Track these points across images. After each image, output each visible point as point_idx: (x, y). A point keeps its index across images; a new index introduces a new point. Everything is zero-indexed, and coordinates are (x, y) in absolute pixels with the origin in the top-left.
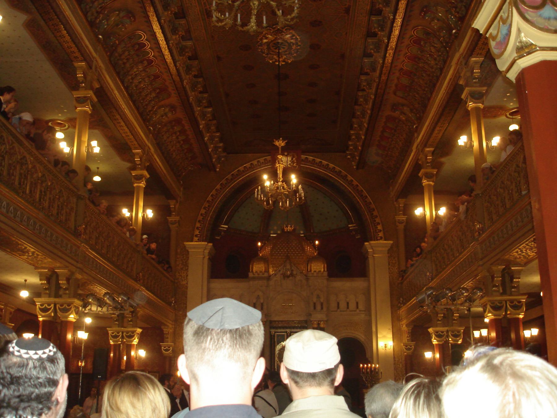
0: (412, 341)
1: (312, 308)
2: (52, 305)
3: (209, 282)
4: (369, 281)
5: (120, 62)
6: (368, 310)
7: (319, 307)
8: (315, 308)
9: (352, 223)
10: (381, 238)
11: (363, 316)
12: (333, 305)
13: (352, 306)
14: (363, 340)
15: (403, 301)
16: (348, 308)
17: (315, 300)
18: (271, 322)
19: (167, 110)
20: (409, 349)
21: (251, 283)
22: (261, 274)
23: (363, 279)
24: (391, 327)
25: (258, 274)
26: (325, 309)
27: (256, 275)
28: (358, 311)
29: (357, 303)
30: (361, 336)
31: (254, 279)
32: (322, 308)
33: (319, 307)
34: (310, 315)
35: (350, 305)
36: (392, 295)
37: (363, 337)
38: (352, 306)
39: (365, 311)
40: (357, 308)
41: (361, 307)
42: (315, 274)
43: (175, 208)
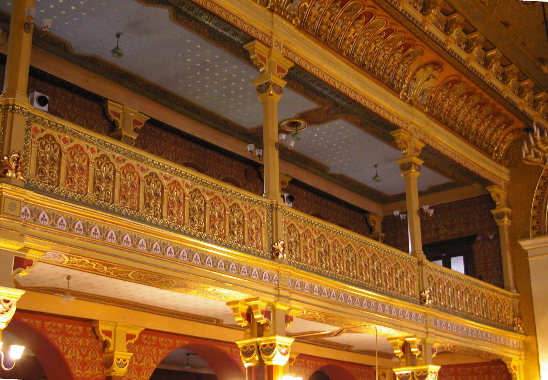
2: (256, 347)
5: (324, 27)
19: (430, 69)
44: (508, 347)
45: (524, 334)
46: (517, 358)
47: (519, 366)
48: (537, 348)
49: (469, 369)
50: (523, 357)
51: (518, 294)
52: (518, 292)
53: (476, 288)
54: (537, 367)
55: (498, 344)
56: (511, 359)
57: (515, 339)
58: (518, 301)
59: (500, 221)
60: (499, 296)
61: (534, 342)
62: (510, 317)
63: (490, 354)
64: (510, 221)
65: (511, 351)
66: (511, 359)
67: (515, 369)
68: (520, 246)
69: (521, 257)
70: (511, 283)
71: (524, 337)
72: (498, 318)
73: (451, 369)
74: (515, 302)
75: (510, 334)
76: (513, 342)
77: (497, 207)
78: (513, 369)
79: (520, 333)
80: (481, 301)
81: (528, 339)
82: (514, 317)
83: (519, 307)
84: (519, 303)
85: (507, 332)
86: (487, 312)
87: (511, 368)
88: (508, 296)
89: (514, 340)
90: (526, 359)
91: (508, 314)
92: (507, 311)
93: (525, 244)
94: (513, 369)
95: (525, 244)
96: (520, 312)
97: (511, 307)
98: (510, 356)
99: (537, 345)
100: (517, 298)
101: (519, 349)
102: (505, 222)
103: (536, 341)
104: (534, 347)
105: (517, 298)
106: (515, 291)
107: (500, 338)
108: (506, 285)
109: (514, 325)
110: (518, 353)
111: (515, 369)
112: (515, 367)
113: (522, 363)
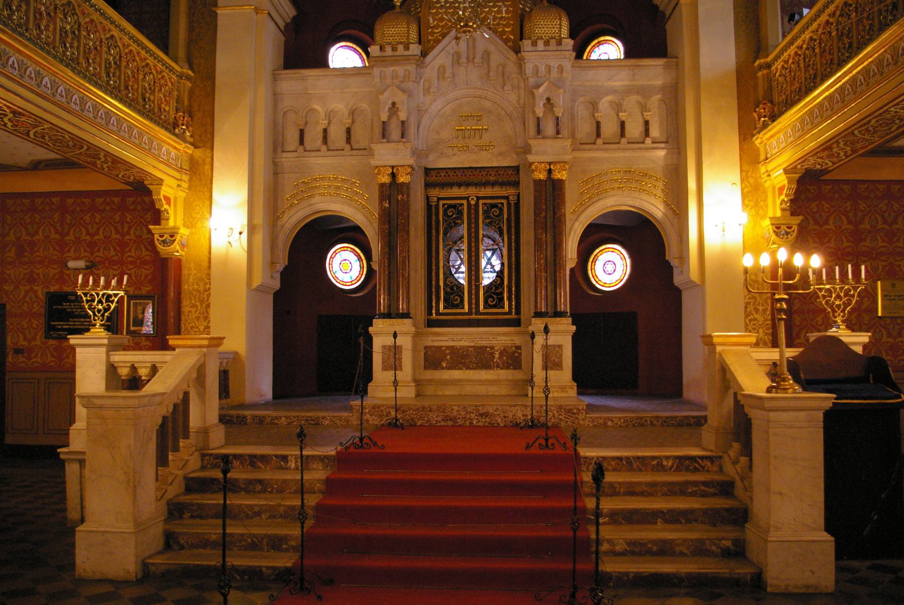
0: (793, 214)
1: (532, 131)
3: (275, 78)
6: (675, 141)
7: (549, 128)
8: (539, 131)
11: (662, 153)
12: (585, 129)
13: (634, 129)
16: (623, 134)
17: (540, 112)
18: (427, 171)
20: (787, 233)
21: (376, 71)
22: (400, 48)
23: (660, 62)
24: (736, 177)
25: (394, 49)
26: (565, 132)
28: (648, 141)
29: (647, 123)
30: (655, 207)
33: (549, 128)
34: (527, 150)
35: (628, 127)
37: (661, 207)
38: (634, 129)
39: (667, 142)
40: (647, 133)
41: (655, 132)
42: (540, 44)
44: (157, 157)
45: (192, 144)
46: (174, 183)
47: (176, 199)
48: (212, 170)
49: (87, 201)
50: (185, 185)
51: (190, 72)
52: (191, 67)
53: (96, 16)
54: (208, 203)
55: (134, 144)
56: (160, 182)
57: (175, 148)
58: (189, 84)
60: (151, 61)
61: (209, 159)
62: (170, 109)
63: (116, 161)
65: (162, 166)
66: (160, 182)
67: (169, 203)
70: (182, 53)
71: (190, 150)
72: (144, 99)
73: (54, 200)
74: (184, 84)
75: (163, 134)
76: (169, 153)
78: (164, 202)
79: (185, 141)
80: (105, 49)
81: (198, 153)
82: (177, 111)
83: (190, 99)
84: (191, 91)
85: (157, 128)
86: (119, 79)
87: (160, 200)
88: (172, 70)
89: (171, 149)
90: (190, 188)
91: (168, 103)
92: (165, 96)
94: (164, 202)
96: (190, 106)
97: (175, 93)
98: (159, 175)
99: (212, 165)
100: (188, 78)
101: (180, 170)
103: (213, 156)
104: (208, 167)
105: (188, 78)
106: (187, 66)
107: (141, 135)
109: (175, 125)
110: (177, 175)
111: (169, 203)
112: (168, 199)
113: (182, 195)
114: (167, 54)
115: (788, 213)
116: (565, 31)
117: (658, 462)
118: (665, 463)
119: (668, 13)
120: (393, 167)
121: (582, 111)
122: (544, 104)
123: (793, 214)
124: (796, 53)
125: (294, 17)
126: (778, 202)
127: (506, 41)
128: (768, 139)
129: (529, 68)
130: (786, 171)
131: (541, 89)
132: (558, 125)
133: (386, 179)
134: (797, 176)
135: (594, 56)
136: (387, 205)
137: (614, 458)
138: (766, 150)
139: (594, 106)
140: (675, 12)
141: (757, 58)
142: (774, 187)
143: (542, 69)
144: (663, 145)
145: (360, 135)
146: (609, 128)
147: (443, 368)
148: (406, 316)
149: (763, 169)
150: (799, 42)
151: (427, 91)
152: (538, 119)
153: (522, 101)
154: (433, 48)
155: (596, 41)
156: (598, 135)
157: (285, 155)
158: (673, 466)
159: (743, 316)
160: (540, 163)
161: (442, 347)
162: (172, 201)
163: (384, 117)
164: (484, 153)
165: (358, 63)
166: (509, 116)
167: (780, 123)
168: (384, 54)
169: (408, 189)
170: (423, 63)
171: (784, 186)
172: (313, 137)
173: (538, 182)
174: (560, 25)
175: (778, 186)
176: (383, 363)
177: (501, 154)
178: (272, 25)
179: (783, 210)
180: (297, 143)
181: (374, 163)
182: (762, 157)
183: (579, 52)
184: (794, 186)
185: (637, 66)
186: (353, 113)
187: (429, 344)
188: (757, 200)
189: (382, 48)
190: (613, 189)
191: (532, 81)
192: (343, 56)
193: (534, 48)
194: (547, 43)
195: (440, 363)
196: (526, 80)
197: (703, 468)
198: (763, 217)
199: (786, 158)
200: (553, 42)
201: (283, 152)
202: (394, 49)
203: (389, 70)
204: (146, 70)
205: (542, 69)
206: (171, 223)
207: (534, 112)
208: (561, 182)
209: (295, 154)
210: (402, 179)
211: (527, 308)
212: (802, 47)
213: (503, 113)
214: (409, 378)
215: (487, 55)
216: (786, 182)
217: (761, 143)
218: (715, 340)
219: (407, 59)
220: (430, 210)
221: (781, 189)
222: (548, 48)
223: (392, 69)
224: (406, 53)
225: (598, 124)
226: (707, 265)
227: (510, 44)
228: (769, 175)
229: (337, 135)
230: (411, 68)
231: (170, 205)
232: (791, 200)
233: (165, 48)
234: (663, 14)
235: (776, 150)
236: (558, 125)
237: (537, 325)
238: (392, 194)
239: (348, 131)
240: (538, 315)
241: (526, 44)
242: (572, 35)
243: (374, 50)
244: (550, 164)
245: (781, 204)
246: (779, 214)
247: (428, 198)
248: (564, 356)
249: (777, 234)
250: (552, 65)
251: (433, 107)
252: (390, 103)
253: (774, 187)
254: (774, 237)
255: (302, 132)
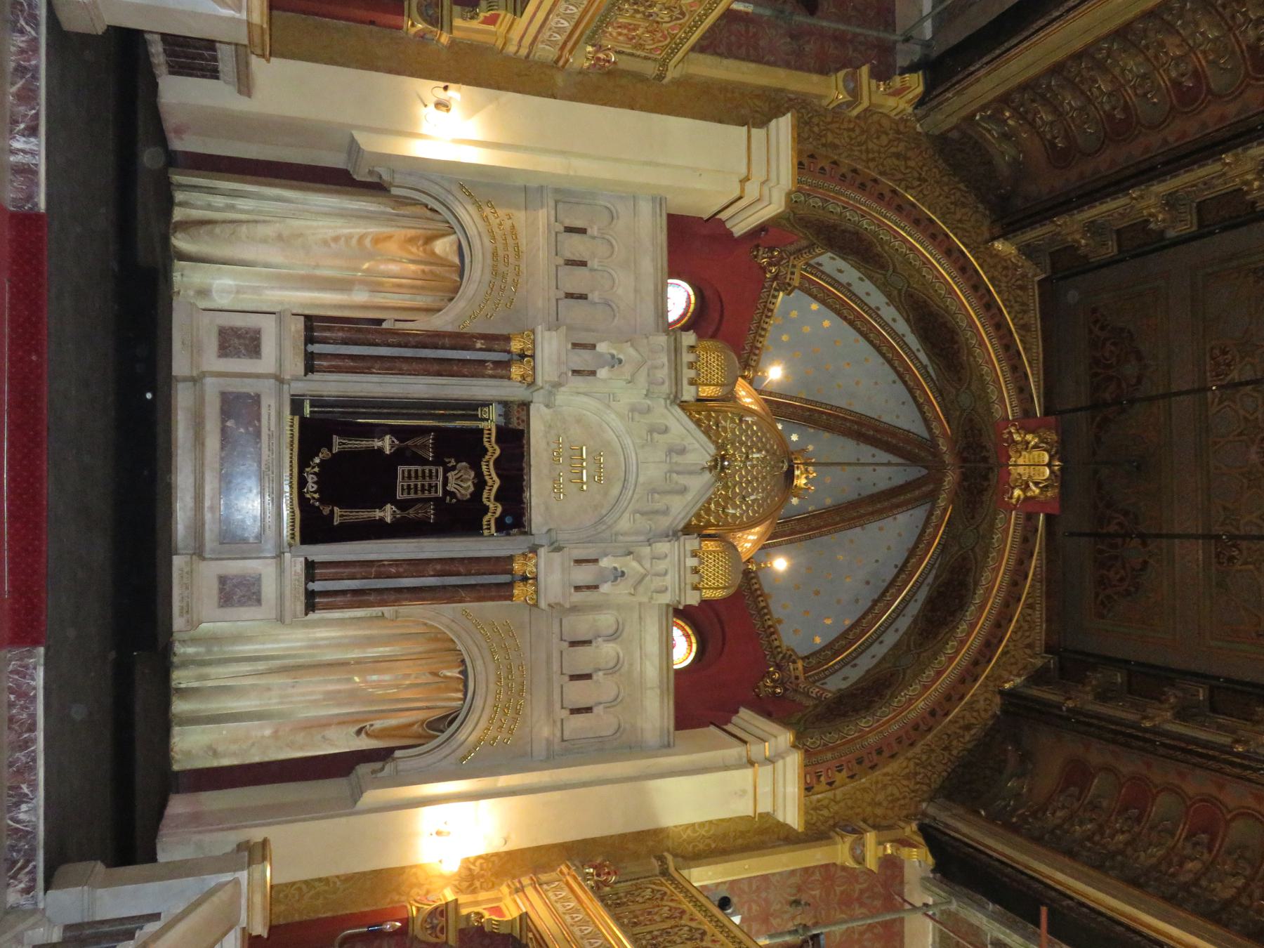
0: (462, 933)
4: (667, 746)
6: (565, 752)
7: (583, 575)
9: (806, 670)
10: (809, 789)
11: (546, 732)
12: (581, 626)
13: (578, 693)
14: (461, 736)
15: (605, 883)
16: (574, 677)
17: (605, 563)
18: (525, 405)
22: (692, 373)
24: (513, 845)
25: (691, 365)
27: (687, 357)
28: (565, 713)
29: (588, 710)
31: (677, 350)
32: (578, 588)
33: (583, 575)
36: (623, 836)
37: (472, 738)
38: (578, 693)
39: (563, 740)
40: (576, 711)
43: (898, 93)
59: (841, 84)
64: (831, 106)
68: (778, 112)
69: (751, 110)
77: (874, 82)
78: (488, 14)
93: (783, 126)
95: (783, 126)
100: (660, 77)
102: (834, 93)
108: (692, 55)
114: (693, 49)
115: (462, 926)
116: (708, 594)
117: (26, 795)
118: (24, 807)
119: (729, 727)
120: (533, 356)
121: (606, 620)
122: (615, 569)
123: (462, 933)
124: (683, 912)
125: (732, 233)
126: (479, 909)
127: (698, 516)
128: (567, 884)
129: (663, 547)
130: (524, 917)
131: (635, 564)
132: (588, 587)
133: (516, 346)
134: (516, 933)
135: (677, 633)
136: (478, 345)
137: (33, 716)
138: (552, 882)
139: (614, 636)
140: (734, 740)
141: (675, 856)
142: (499, 899)
143: (661, 566)
144: (558, 734)
145: (576, 311)
146: (582, 659)
147: (223, 421)
148: (310, 368)
149: (526, 881)
150: (699, 916)
151: (633, 409)
152: (596, 561)
153: (621, 538)
154: (690, 416)
155: (690, 632)
156: (574, 644)
157: (552, 203)
158: (18, 822)
159: (305, 878)
160: (536, 565)
161: (259, 421)
162: (492, 28)
163: (602, 347)
164: (549, 485)
165: (672, 317)
166: (601, 520)
167: (591, 900)
168: (684, 350)
169: (502, 377)
170: (673, 402)
171: (502, 915)
172: (575, 246)
173: (511, 559)
174: (717, 589)
175: (501, 905)
176: (232, 328)
177: (547, 508)
178: (725, 201)
179: (468, 916)
180: (568, 223)
181: (539, 329)
182: (544, 877)
183: (684, 614)
184: (504, 930)
185: (662, 693)
186: (607, 304)
187: (265, 402)
188: (483, 876)
189: (692, 348)
190: (498, 668)
191: (646, 550)
192: (679, 297)
193: (688, 554)
194: (695, 571)
195: (229, 418)
196: (649, 542)
197: (14, 877)
198: (459, 890)
199: (544, 920)
200: (696, 578)
201: (556, 202)
202: (691, 365)
203: (664, 359)
204: (677, 12)
205: (661, 566)
206: (458, 22)
207: (606, 555)
208: (510, 597)
209: (553, 219)
210: (516, 371)
211: (323, 552)
212: (692, 920)
213: (604, 512)
214: (206, 368)
215: (683, 490)
216: (508, 918)
217: (561, 872)
218: (257, 868)
219: (677, 381)
220: (471, 408)
221: (497, 911)
222: (689, 571)
223: (665, 360)
224: (685, 382)
225: (588, 642)
226: (386, 814)
227: (694, 522)
228: (517, 891)
229: (575, 280)
230: (666, 388)
231: (483, 22)
232: (481, 928)
233: (700, 48)
234: (728, 721)
235: (553, 898)
236: (588, 587)
237: (295, 566)
238: (494, 351)
239: (583, 297)
240: (310, 566)
241: (692, 543)
242: (705, 603)
243: (689, 338)
244: (535, 578)
245: (477, 914)
246: (464, 912)
247: (486, 404)
248: (243, 609)
249: (433, 913)
250: (668, 577)
251: (613, 416)
252: (621, 356)
253: (499, 899)
254: (428, 908)
255: (583, 231)
